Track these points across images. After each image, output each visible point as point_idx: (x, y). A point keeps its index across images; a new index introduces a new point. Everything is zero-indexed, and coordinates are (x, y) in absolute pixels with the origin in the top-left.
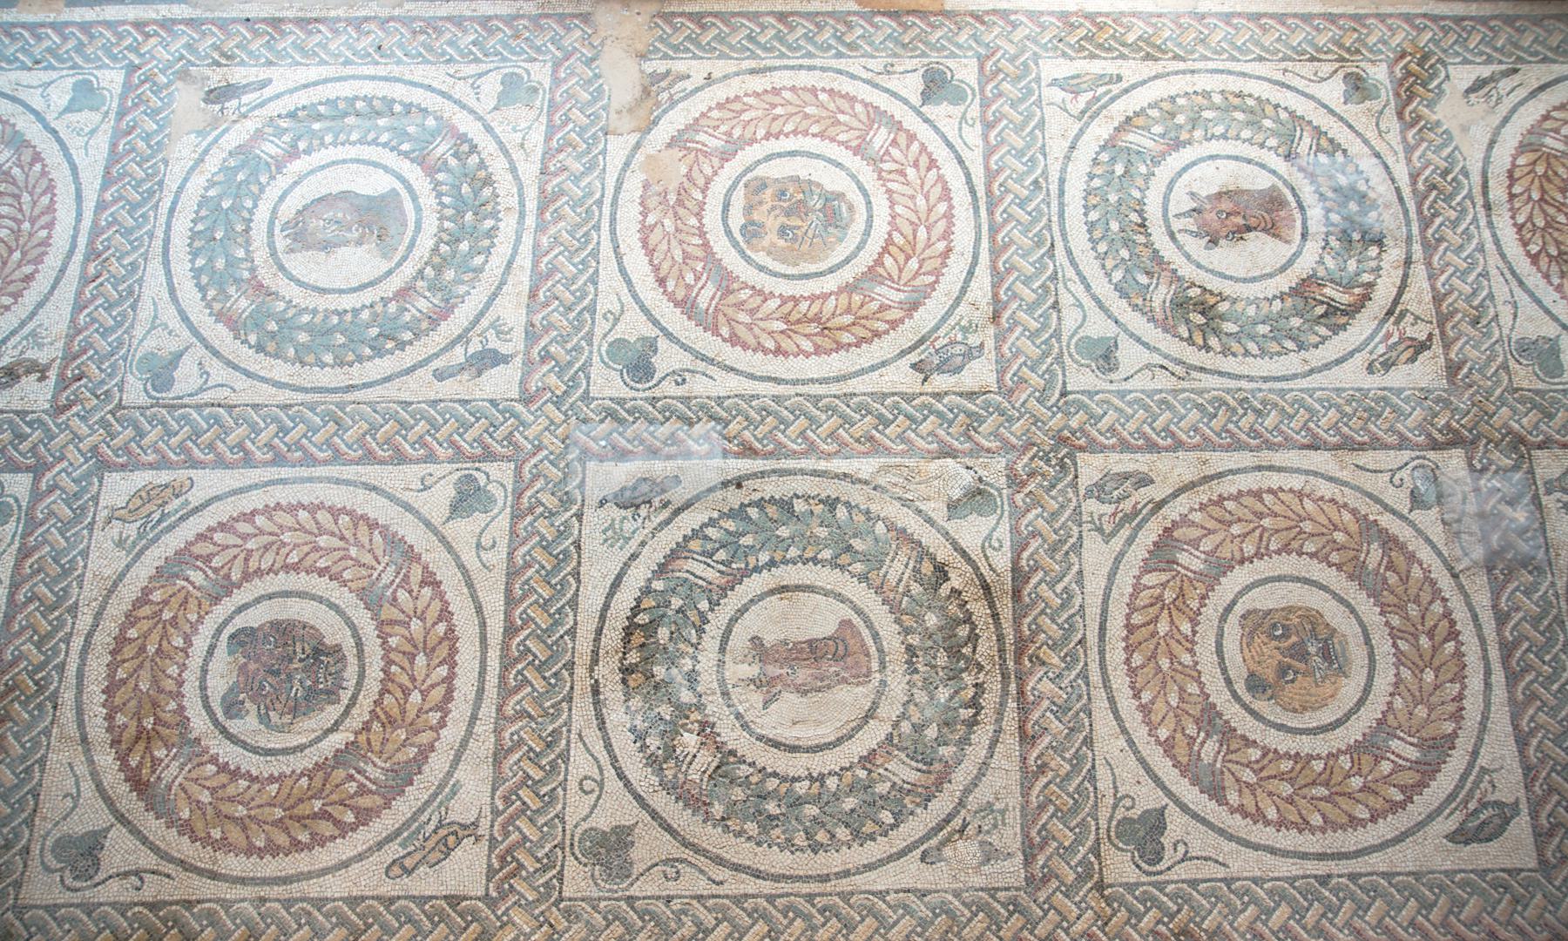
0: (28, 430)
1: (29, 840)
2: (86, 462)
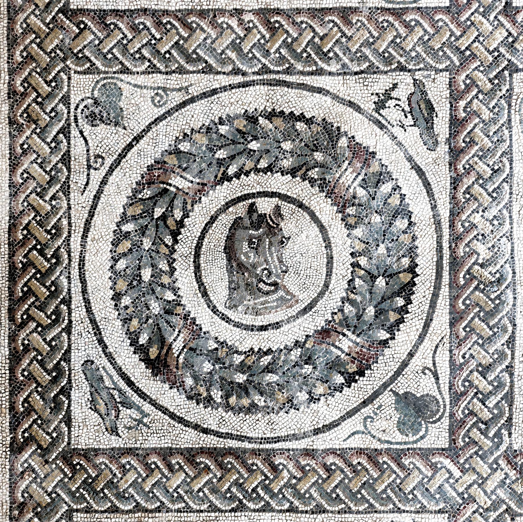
0: (491, 435)
1: (123, 511)
2: (459, 494)
